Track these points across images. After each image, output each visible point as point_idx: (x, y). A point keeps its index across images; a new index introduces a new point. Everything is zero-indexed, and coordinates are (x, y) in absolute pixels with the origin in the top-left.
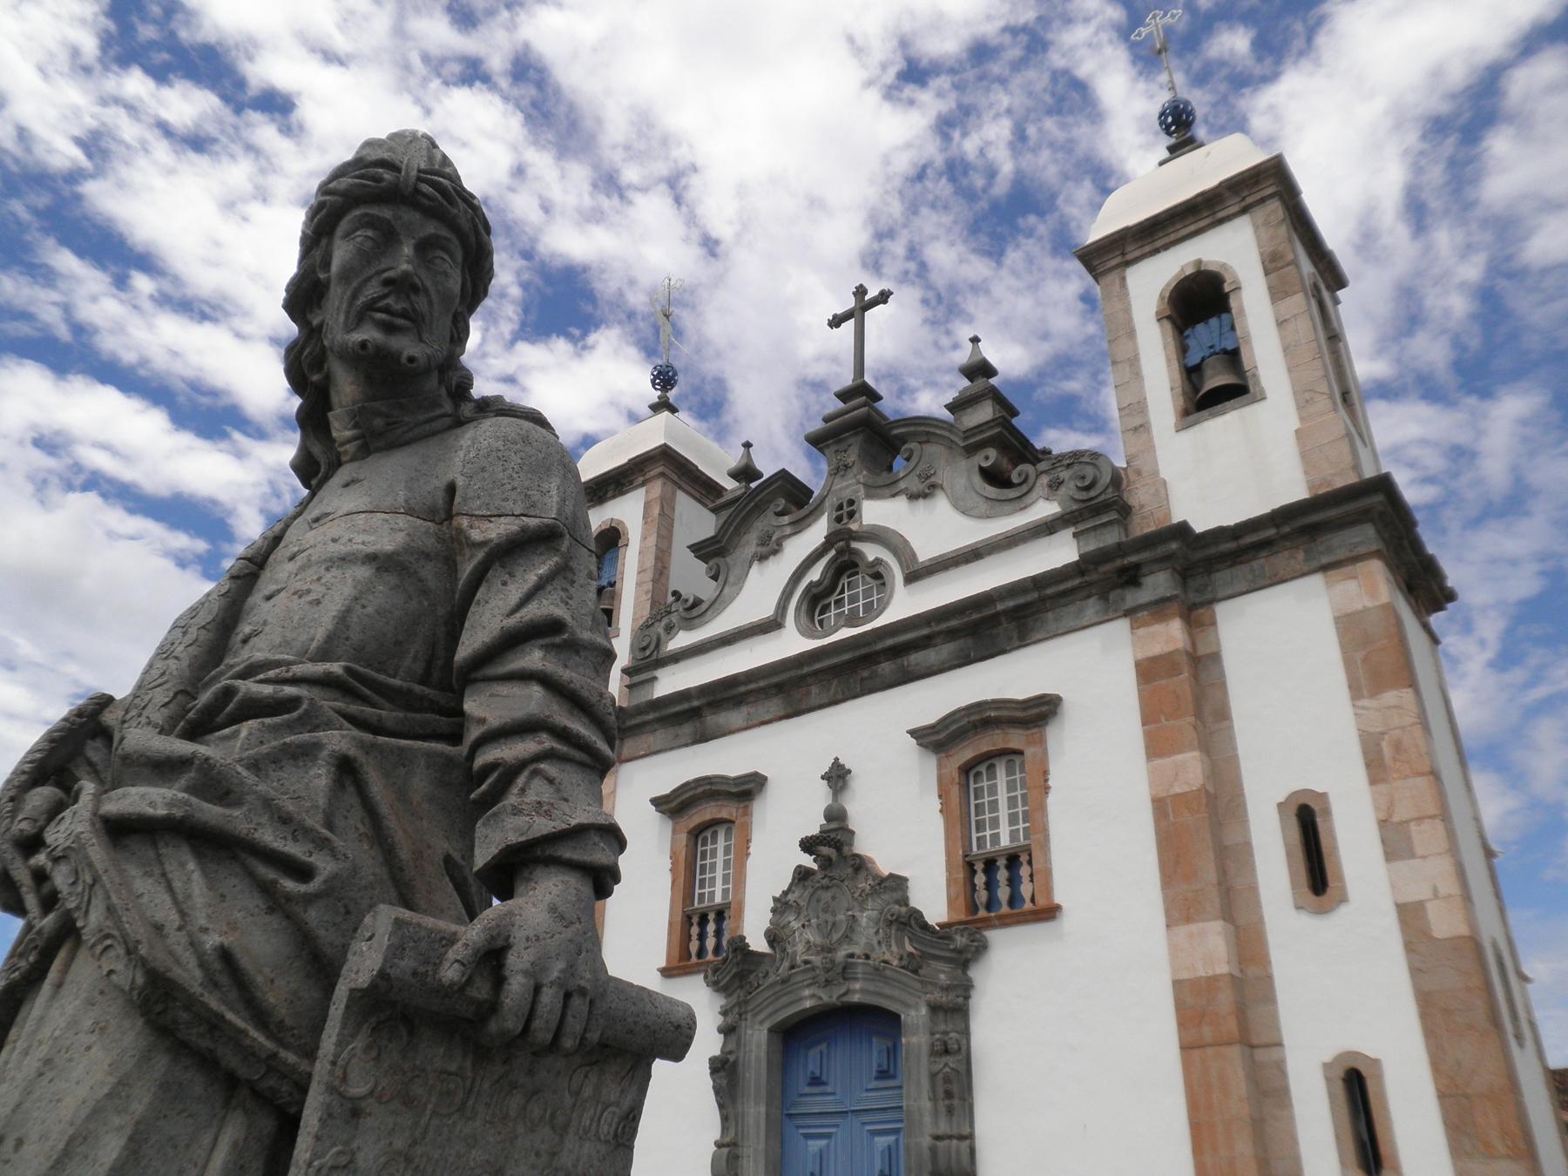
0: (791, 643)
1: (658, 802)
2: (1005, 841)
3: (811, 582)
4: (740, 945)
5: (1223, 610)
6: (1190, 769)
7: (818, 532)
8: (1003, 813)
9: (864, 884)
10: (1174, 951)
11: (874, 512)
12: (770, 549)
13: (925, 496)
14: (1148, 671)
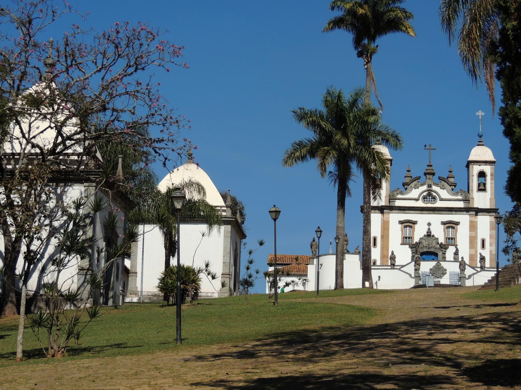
0: (420, 204)
1: (399, 221)
2: (450, 236)
3: (424, 195)
4: (416, 242)
5: (478, 216)
6: (474, 234)
7: (425, 188)
8: (450, 233)
9: (434, 238)
10: (470, 252)
11: (434, 188)
12: (416, 187)
13: (443, 189)
14: (471, 222)
